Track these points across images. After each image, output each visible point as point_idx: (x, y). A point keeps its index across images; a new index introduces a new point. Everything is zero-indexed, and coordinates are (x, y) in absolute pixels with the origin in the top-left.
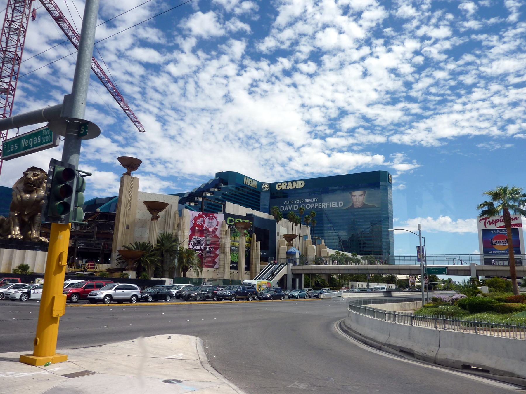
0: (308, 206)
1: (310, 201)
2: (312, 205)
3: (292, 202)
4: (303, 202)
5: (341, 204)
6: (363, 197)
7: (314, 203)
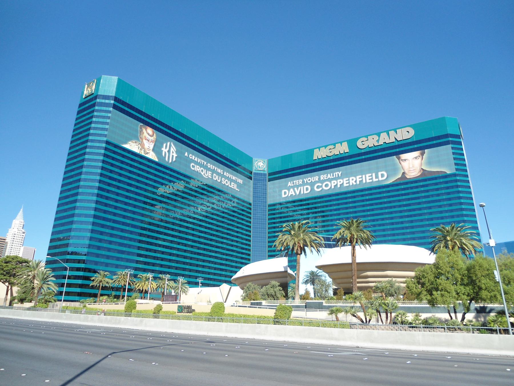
0: (326, 185)
1: (329, 176)
2: (333, 183)
3: (301, 183)
4: (317, 179)
5: (382, 176)
6: (420, 159)
7: (336, 179)
